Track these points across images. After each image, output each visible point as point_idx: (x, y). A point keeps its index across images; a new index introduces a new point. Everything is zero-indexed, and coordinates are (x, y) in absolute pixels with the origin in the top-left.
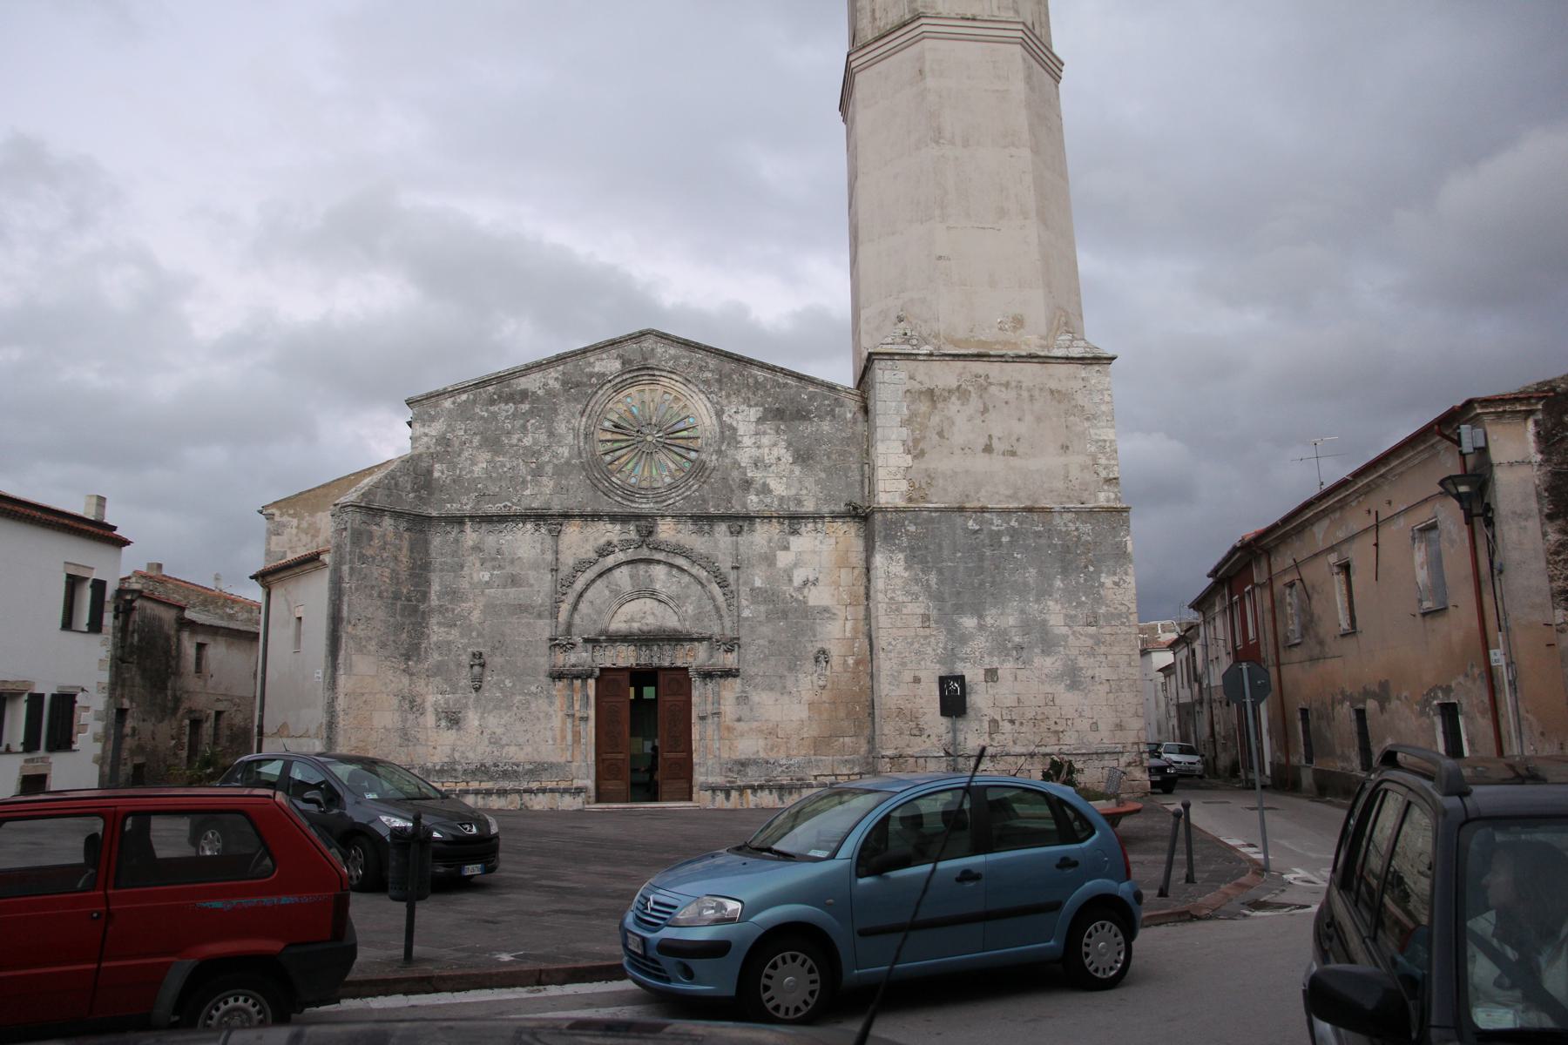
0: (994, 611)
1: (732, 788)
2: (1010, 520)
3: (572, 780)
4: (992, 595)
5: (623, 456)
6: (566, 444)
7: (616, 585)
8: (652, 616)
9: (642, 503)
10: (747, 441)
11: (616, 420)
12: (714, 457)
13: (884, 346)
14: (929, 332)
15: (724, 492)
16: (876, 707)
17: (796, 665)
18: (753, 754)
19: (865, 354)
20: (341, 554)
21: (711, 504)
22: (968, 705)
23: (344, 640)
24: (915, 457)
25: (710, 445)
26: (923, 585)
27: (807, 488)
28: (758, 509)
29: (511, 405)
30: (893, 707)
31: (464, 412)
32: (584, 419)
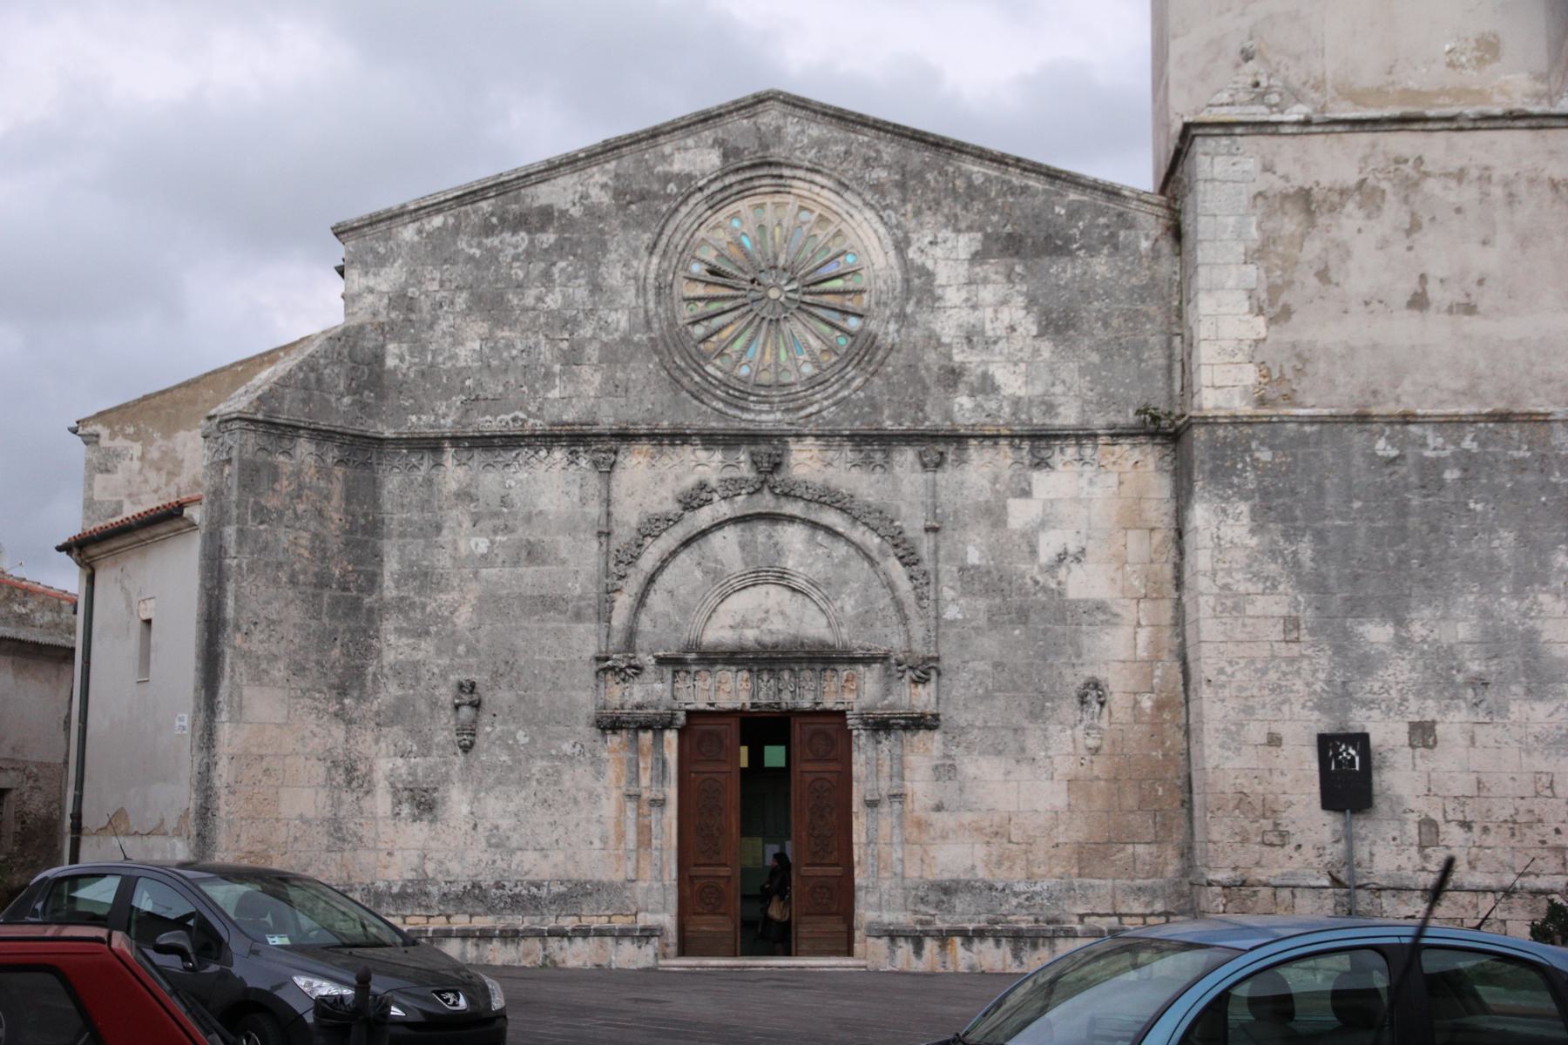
0: (1427, 613)
1: (926, 934)
2: (1462, 438)
3: (636, 915)
4: (1424, 580)
5: (724, 327)
7: (716, 561)
8: (780, 617)
9: (761, 412)
10: (953, 296)
11: (713, 261)
12: (892, 327)
13: (1215, 110)
14: (1304, 78)
15: (911, 390)
16: (1195, 790)
17: (1043, 708)
18: (965, 872)
19: (1177, 127)
20: (221, 507)
21: (887, 412)
22: (1376, 789)
23: (228, 660)
24: (1272, 321)
25: (886, 304)
26: (1285, 562)
27: (1064, 382)
28: (972, 421)
29: (523, 234)
30: (1229, 790)
31: (438, 249)
32: (655, 260)
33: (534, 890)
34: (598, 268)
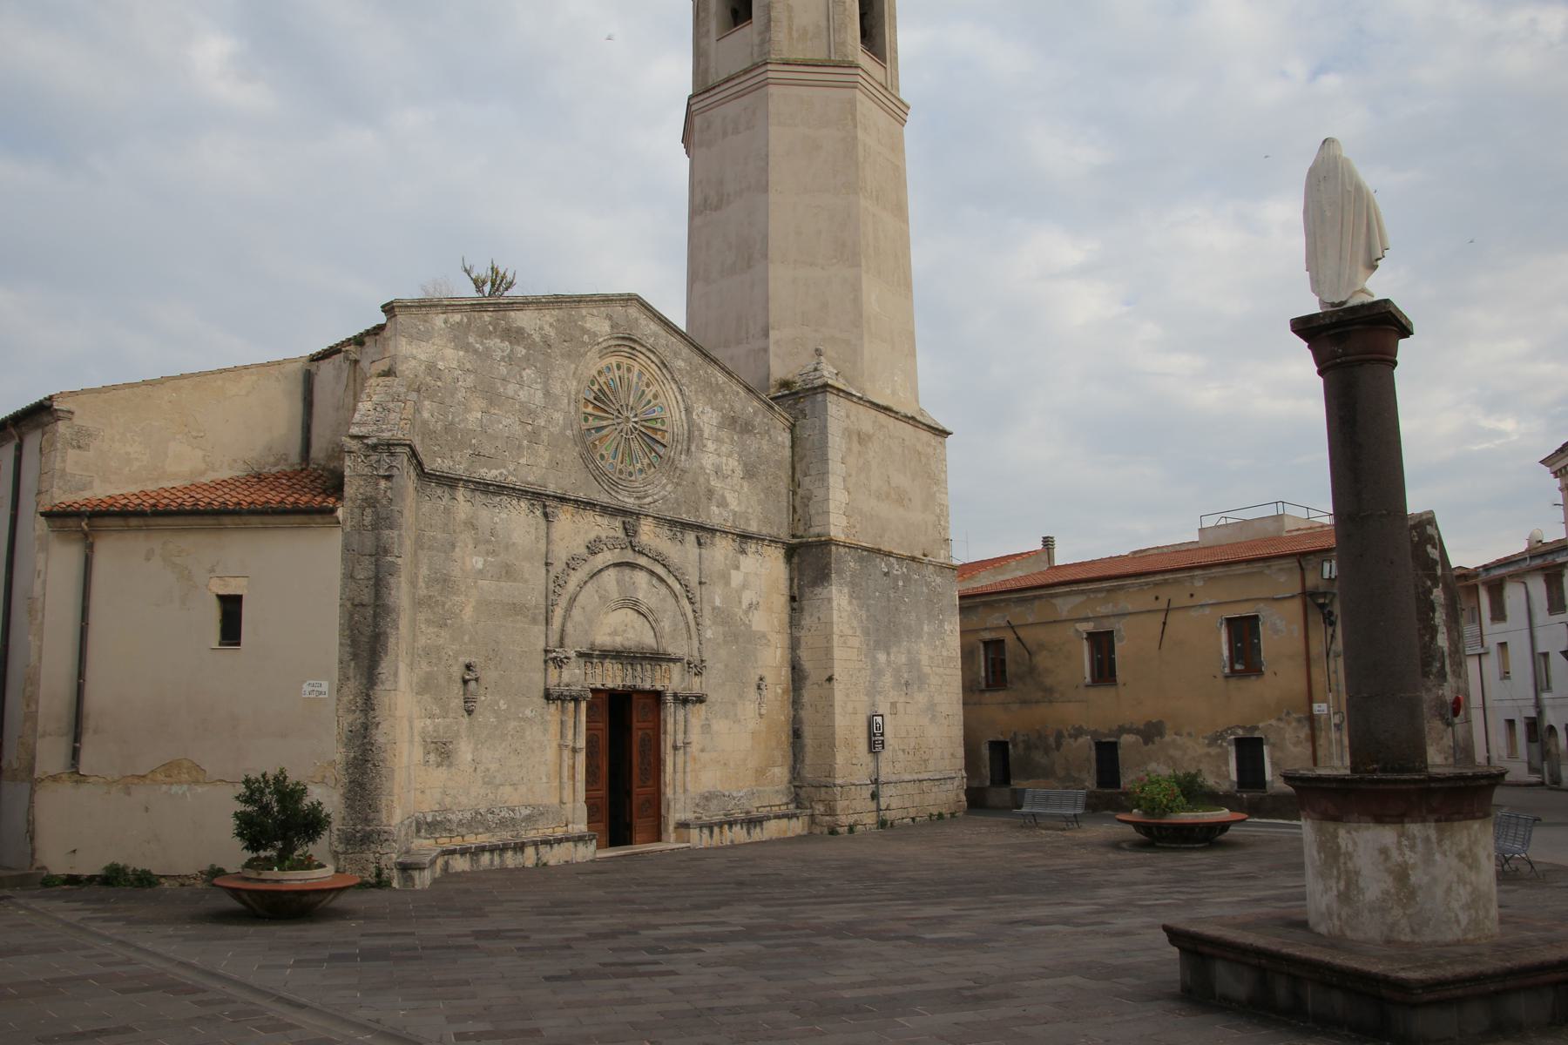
3: (567, 825)
6: (561, 409)
7: (605, 590)
8: (632, 630)
9: (624, 496)
10: (711, 446)
17: (744, 692)
21: (684, 509)
33: (512, 814)
34: (548, 379)
